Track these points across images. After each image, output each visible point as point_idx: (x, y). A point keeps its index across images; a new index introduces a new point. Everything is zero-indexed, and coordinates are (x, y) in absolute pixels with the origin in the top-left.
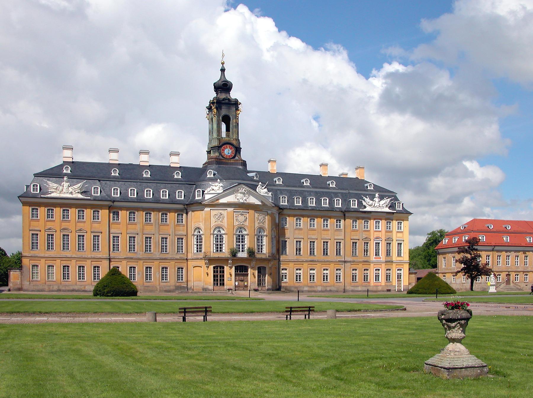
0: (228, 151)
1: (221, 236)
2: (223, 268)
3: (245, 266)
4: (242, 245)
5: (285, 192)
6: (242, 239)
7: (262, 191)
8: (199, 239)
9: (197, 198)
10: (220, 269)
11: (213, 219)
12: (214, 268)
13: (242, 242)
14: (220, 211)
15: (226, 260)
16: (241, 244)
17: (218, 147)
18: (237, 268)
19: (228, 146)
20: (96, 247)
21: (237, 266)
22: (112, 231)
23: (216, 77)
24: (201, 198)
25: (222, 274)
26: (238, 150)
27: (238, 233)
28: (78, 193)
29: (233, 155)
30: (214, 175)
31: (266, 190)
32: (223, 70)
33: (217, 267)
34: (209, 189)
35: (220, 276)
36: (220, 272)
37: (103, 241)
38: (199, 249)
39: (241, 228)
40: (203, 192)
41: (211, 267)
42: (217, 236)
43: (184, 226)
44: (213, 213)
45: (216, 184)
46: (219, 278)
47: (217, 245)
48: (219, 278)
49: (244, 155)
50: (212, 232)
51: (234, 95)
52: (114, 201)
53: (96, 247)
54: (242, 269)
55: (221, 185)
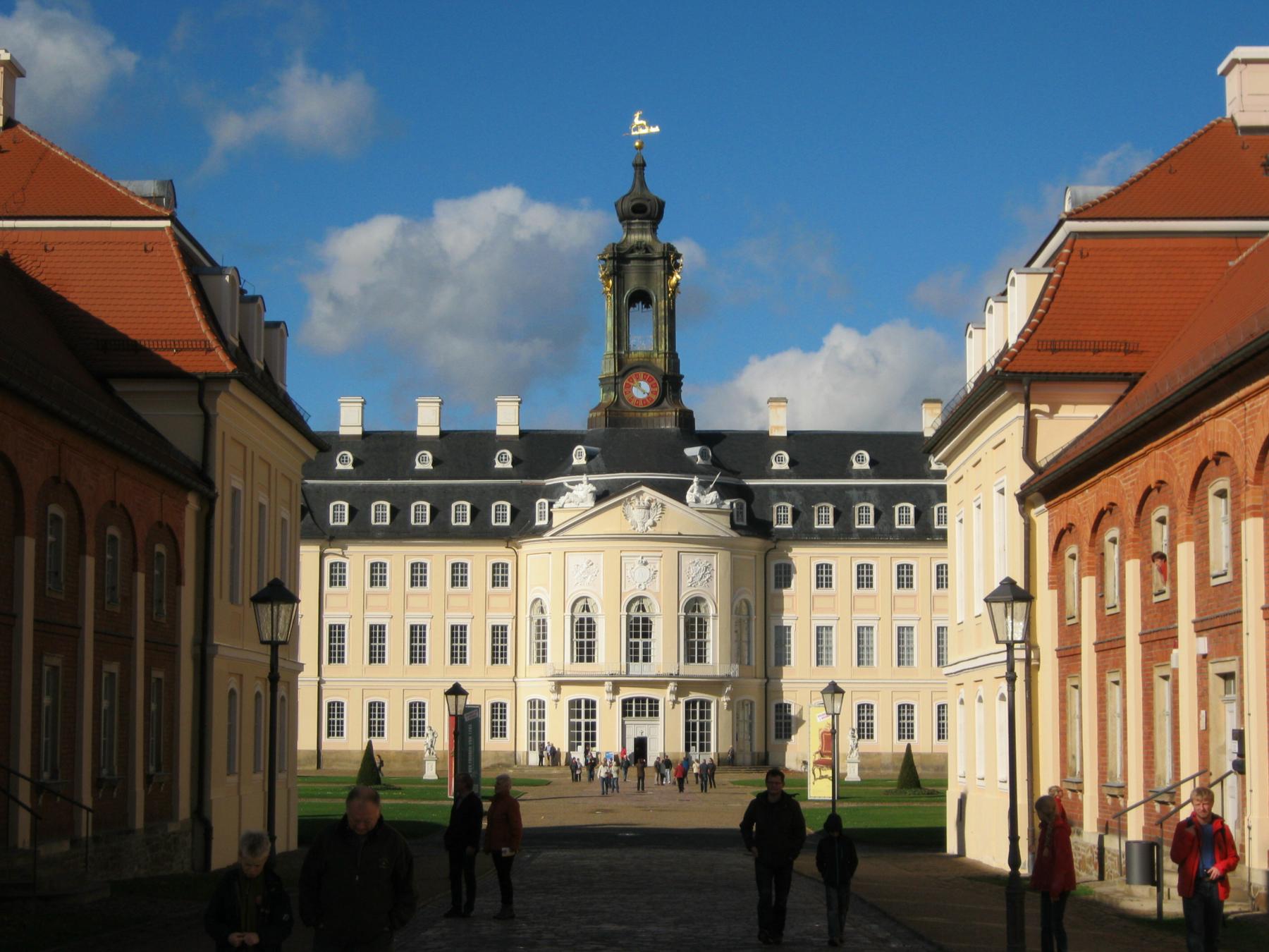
0: (642, 390)
3: (651, 700)
4: (646, 645)
5: (793, 493)
7: (701, 497)
9: (538, 523)
13: (645, 635)
14: (589, 556)
16: (641, 641)
18: (626, 704)
21: (630, 700)
22: (326, 613)
23: (623, 184)
24: (545, 522)
25: (590, 720)
26: (671, 383)
27: (633, 613)
29: (655, 398)
30: (590, 457)
31: (713, 495)
32: (640, 166)
35: (587, 725)
36: (587, 717)
38: (541, 656)
39: (638, 602)
40: (551, 505)
42: (582, 620)
46: (583, 732)
48: (583, 732)
49: (689, 396)
50: (568, 612)
51: (666, 232)
52: (332, 539)
54: (644, 707)
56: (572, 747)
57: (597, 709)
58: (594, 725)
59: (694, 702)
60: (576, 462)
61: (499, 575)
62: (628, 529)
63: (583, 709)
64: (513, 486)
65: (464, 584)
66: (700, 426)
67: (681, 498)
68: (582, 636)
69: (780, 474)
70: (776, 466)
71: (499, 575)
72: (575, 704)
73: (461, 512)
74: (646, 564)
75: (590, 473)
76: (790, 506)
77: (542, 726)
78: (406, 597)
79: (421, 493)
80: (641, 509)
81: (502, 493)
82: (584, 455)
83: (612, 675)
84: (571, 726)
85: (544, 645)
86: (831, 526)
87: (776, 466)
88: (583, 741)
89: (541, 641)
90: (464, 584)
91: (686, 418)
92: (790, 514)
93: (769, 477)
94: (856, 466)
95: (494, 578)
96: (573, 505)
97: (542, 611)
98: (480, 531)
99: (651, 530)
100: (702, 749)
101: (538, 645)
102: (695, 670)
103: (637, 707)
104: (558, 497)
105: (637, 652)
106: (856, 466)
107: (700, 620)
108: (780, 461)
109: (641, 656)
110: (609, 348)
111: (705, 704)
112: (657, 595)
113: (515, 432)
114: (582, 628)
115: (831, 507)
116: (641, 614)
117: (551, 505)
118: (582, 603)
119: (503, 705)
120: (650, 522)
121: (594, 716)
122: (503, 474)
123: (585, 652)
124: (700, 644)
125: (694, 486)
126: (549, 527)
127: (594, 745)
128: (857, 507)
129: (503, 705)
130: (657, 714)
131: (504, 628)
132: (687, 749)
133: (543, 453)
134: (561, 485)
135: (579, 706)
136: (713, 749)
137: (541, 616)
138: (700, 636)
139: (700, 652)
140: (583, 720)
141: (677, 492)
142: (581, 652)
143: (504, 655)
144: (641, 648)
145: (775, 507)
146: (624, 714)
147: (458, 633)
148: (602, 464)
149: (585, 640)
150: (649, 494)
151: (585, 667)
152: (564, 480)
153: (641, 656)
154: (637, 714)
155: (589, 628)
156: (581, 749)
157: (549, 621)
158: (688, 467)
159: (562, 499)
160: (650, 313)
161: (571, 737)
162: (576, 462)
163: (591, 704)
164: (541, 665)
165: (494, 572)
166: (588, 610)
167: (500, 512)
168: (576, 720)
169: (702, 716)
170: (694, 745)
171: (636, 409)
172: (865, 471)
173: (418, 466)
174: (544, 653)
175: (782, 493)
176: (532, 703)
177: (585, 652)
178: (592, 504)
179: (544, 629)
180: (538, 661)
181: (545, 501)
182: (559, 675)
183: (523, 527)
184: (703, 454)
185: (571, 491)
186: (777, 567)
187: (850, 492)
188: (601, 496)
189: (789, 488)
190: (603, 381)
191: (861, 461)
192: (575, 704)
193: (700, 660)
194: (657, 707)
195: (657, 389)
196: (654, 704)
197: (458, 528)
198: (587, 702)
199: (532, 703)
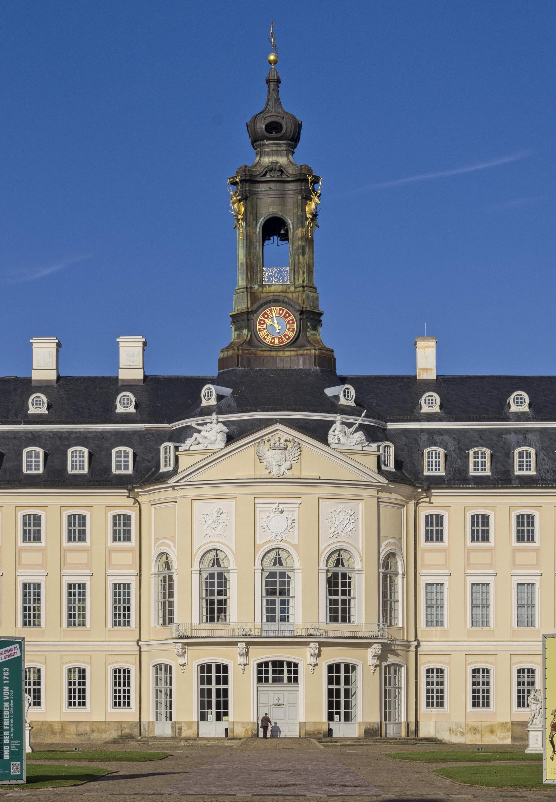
3: (289, 664)
4: (283, 602)
5: (446, 437)
6: (283, 583)
8: (167, 585)
9: (163, 469)
10: (218, 671)
13: (282, 593)
16: (278, 598)
17: (248, 313)
18: (262, 668)
21: (266, 664)
24: (171, 468)
25: (222, 687)
29: (292, 335)
30: (220, 398)
35: (218, 691)
36: (218, 683)
40: (177, 448)
42: (211, 576)
46: (214, 699)
47: (212, 603)
48: (214, 699)
54: (282, 672)
56: (203, 717)
57: (230, 674)
58: (226, 691)
59: (338, 666)
60: (204, 403)
61: (121, 529)
62: (262, 473)
63: (214, 675)
64: (135, 433)
65: (82, 539)
66: (341, 371)
67: (325, 441)
68: (212, 593)
69: (430, 417)
70: (425, 409)
72: (205, 668)
73: (78, 460)
74: (282, 512)
75: (220, 412)
76: (442, 451)
77: (170, 694)
78: (19, 552)
79: (34, 439)
80: (277, 448)
81: (123, 438)
82: (214, 395)
83: (245, 636)
85: (171, 604)
86: (488, 473)
87: (425, 409)
88: (214, 710)
89: (167, 600)
90: (82, 539)
91: (327, 360)
92: (442, 460)
93: (419, 421)
94: (514, 408)
95: (115, 532)
96: (200, 447)
97: (169, 568)
98: (100, 478)
99: (288, 474)
100: (347, 718)
101: (164, 604)
102: (339, 629)
103: (274, 672)
104: (183, 441)
105: (273, 611)
106: (514, 408)
107: (344, 575)
108: (430, 403)
109: (278, 615)
110: (242, 282)
111: (350, 668)
112: (293, 545)
113: (139, 375)
114: (212, 585)
115: (488, 452)
116: (278, 569)
117: (177, 448)
118: (211, 555)
119: (127, 672)
120: (288, 464)
121: (226, 682)
122: (126, 418)
123: (215, 609)
124: (344, 602)
125: (337, 426)
126: (175, 471)
127: (226, 714)
128: (517, 451)
129: (127, 672)
130: (296, 680)
131: (127, 586)
132: (330, 718)
133: (170, 399)
134: (189, 427)
135: (209, 671)
136: (359, 719)
137: (167, 573)
138: (344, 593)
139: (344, 611)
140: (214, 687)
141: (319, 432)
142: (212, 611)
143: (127, 616)
144: (278, 607)
145: (426, 451)
146: (259, 680)
147: (76, 592)
148: (233, 404)
149: (216, 598)
150: (285, 433)
152: (192, 422)
153: (278, 615)
154: (274, 680)
155: (220, 584)
156: (212, 717)
157: (175, 577)
158: (332, 406)
159: (189, 441)
160: (288, 247)
161: (202, 705)
162: (204, 403)
163: (223, 669)
164: (167, 627)
165: (115, 524)
166: (219, 565)
167: (122, 460)
168: (206, 687)
169: (347, 682)
170: (338, 713)
171: (271, 348)
172: (524, 413)
173: (32, 410)
174: (171, 613)
175: (433, 437)
176: (158, 667)
177: (215, 609)
178: (222, 445)
179: (171, 587)
180: (164, 623)
181: (171, 445)
183: (148, 474)
184: (346, 393)
185: (199, 432)
186: (427, 517)
187: (508, 436)
189: (440, 432)
190: (236, 318)
191: (519, 402)
192: (205, 668)
193: (344, 620)
194: (296, 672)
195: (294, 326)
196: (293, 668)
197: (75, 476)
198: (218, 666)
199: (158, 667)
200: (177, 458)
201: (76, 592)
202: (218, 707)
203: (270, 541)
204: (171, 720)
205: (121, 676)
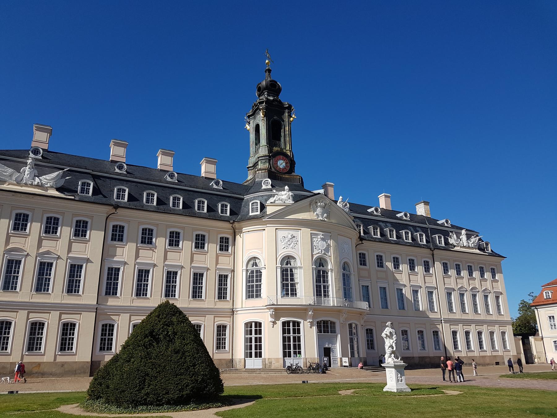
0: (282, 164)
1: (291, 270)
2: (298, 324)
4: (324, 287)
9: (251, 214)
10: (294, 326)
11: (281, 245)
12: (284, 324)
13: (324, 282)
15: (302, 311)
19: (282, 157)
20: (72, 287)
28: (51, 187)
33: (288, 322)
34: (272, 200)
35: (294, 338)
36: (294, 333)
37: (91, 278)
41: (279, 324)
43: (229, 256)
44: (281, 234)
45: (283, 193)
53: (72, 287)
55: (291, 193)
71: (225, 245)
84: (284, 339)
96: (281, 202)
129: (225, 327)
147: (198, 278)
151: (289, 301)
176: (248, 325)
182: (273, 305)
188: (297, 199)
199: (248, 325)
200: (263, 207)
201: (198, 278)
202: (295, 348)
203: (319, 253)
204: (260, 356)
205: (221, 329)
